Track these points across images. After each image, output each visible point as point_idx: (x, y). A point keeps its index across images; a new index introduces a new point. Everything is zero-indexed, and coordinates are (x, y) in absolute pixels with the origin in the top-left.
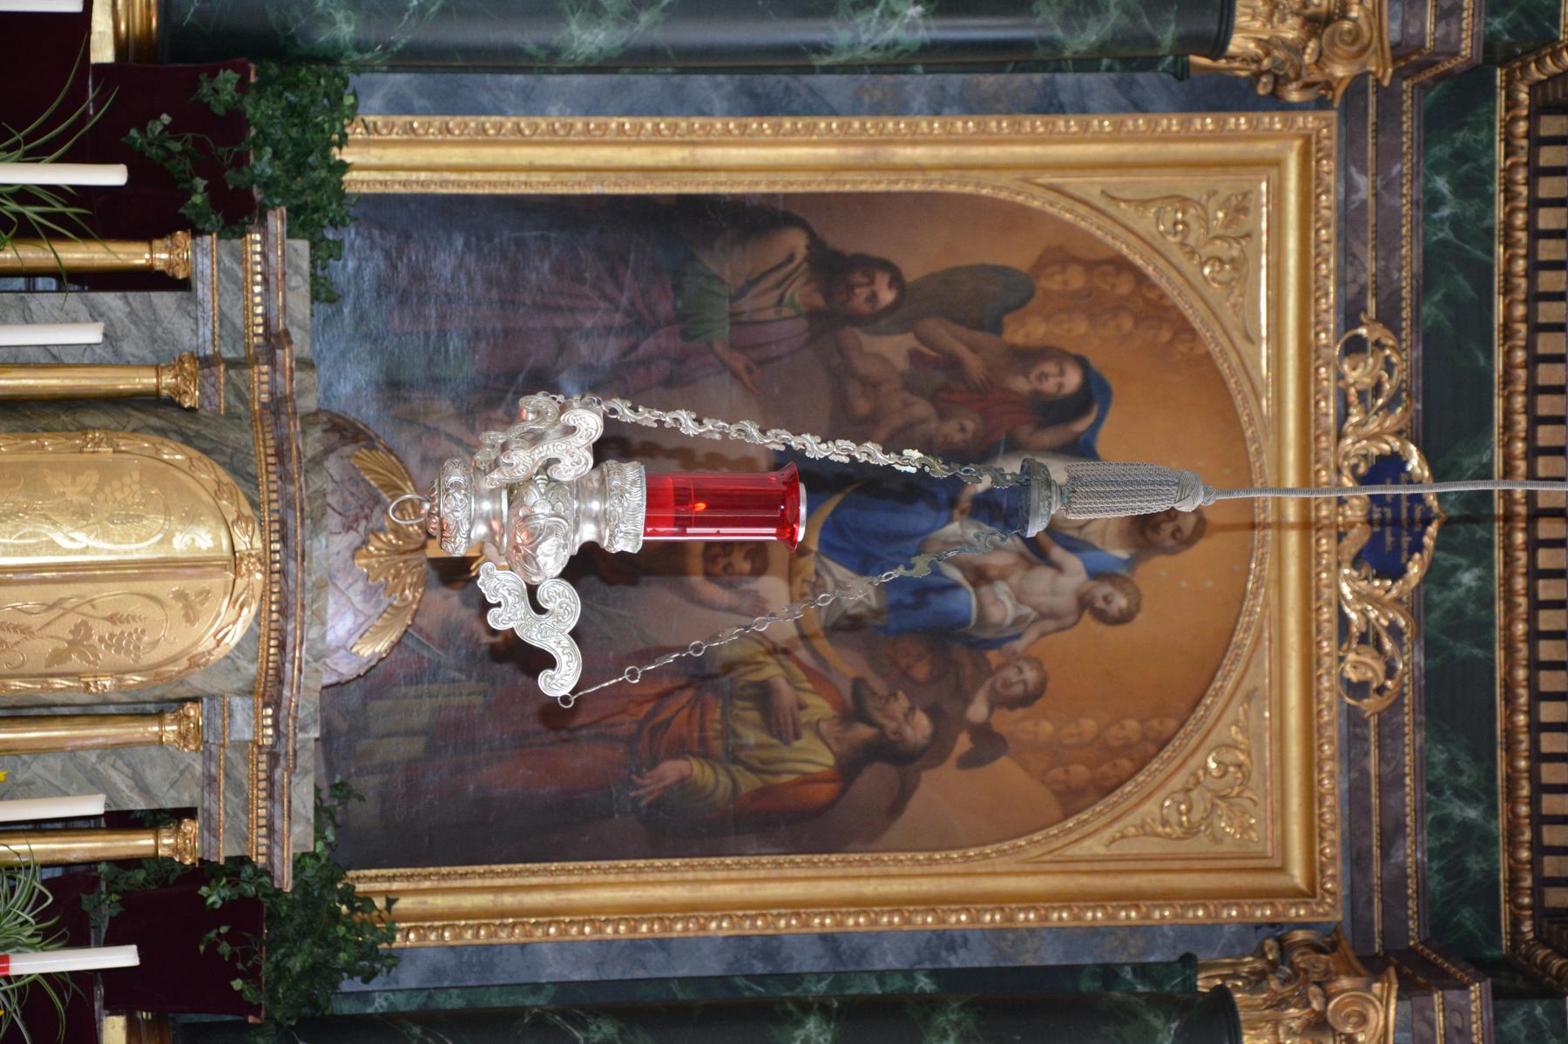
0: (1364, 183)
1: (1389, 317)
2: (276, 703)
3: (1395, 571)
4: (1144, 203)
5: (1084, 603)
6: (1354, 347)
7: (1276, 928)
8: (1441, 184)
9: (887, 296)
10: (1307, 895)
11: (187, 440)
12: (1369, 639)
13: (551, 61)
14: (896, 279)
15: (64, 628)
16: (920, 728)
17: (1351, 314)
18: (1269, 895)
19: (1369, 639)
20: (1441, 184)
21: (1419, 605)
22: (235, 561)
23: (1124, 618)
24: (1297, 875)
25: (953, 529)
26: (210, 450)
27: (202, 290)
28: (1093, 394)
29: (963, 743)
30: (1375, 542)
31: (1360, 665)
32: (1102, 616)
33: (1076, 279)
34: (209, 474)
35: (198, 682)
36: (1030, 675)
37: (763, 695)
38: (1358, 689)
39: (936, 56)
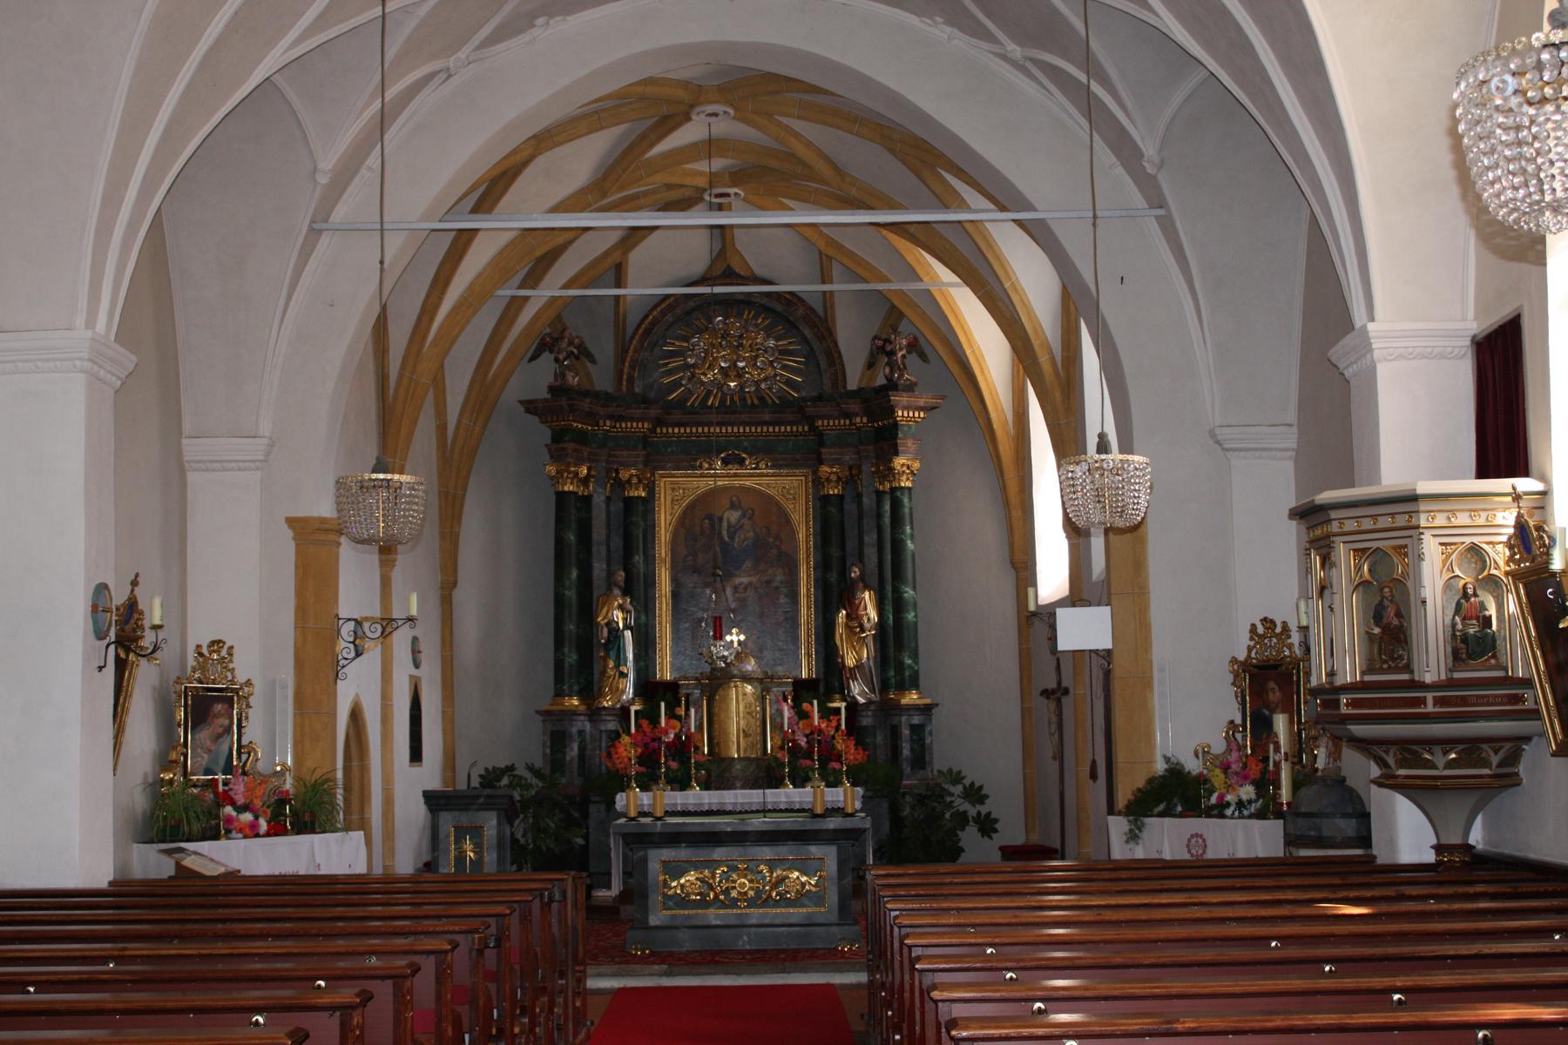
0: (669, 465)
1: (696, 460)
2: (762, 679)
3: (744, 459)
4: (673, 509)
5: (750, 519)
6: (701, 467)
7: (813, 481)
8: (669, 450)
9: (690, 558)
10: (806, 477)
11: (715, 695)
12: (757, 464)
13: (646, 625)
14: (686, 556)
15: (747, 716)
16: (774, 551)
17: (694, 468)
18: (806, 483)
19: (757, 464)
20: (669, 450)
21: (750, 455)
22: (736, 687)
23: (753, 511)
24: (803, 478)
25: (736, 545)
26: (716, 691)
27: (689, 692)
28: (710, 517)
29: (778, 543)
30: (738, 463)
31: (762, 465)
32: (753, 515)
33: (687, 520)
34: (721, 692)
35: (759, 692)
36: (764, 530)
37: (768, 582)
38: (767, 465)
39: (645, 554)
